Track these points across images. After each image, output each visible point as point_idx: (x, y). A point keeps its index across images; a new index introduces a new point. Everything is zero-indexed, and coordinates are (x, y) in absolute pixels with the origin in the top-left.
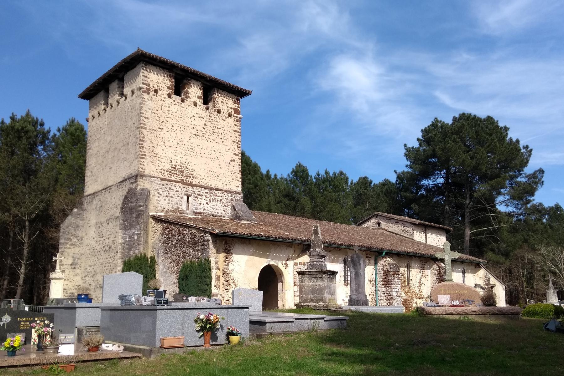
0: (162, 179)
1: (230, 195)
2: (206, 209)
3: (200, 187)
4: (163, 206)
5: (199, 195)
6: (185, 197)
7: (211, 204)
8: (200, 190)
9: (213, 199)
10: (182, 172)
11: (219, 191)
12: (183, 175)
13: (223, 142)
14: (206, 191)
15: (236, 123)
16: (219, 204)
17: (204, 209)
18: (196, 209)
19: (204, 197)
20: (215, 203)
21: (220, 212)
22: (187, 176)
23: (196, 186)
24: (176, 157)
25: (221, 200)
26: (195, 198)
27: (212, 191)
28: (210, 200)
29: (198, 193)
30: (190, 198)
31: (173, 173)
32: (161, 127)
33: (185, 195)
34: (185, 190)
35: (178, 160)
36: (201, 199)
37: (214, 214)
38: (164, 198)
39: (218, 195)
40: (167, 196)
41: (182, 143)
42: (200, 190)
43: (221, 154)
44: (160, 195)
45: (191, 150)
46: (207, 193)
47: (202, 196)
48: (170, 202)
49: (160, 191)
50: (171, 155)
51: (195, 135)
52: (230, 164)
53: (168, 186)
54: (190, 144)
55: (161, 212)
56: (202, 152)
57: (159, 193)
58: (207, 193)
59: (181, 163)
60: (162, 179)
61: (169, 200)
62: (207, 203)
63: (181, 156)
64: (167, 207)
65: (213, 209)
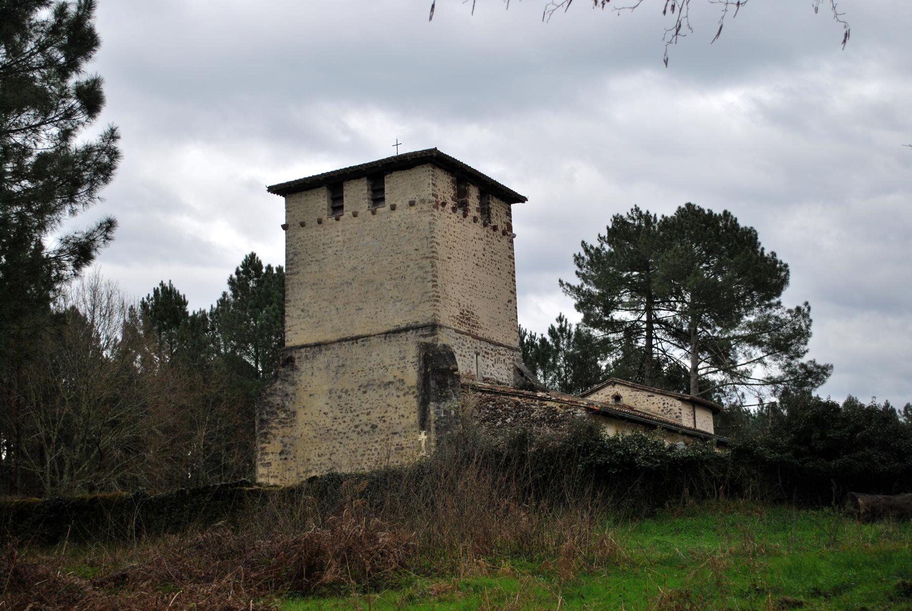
0: (457, 331)
1: (511, 353)
12: (469, 324)
14: (492, 347)
16: (503, 366)
17: (491, 374)
19: (490, 355)
20: (499, 365)
22: (473, 326)
27: (497, 348)
36: (488, 358)
37: (500, 380)
39: (502, 352)
41: (466, 277)
47: (488, 354)
50: (459, 296)
51: (477, 264)
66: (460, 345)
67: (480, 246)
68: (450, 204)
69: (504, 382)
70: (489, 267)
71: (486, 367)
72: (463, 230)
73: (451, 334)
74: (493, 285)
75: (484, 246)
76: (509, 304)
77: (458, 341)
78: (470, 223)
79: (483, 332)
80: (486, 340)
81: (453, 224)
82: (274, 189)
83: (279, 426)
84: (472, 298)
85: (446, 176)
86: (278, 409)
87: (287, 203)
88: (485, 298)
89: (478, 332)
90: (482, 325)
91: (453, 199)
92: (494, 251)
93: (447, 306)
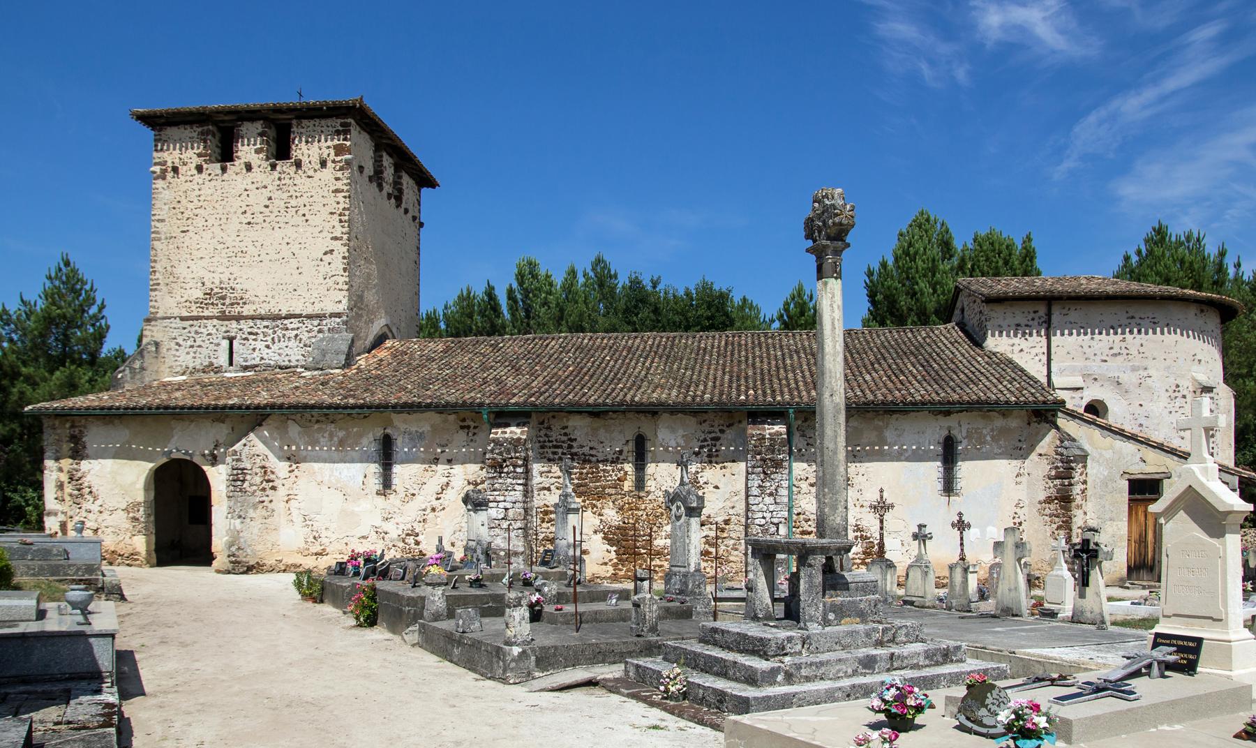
0: (183, 319)
1: (316, 323)
2: (265, 357)
3: (253, 319)
4: (184, 364)
5: (250, 333)
6: (225, 343)
7: (275, 347)
8: (252, 324)
9: (279, 337)
10: (223, 298)
11: (292, 320)
12: (224, 304)
13: (307, 221)
14: (265, 323)
15: (339, 174)
16: (292, 343)
17: (262, 358)
18: (244, 361)
19: (261, 337)
20: (282, 344)
21: (293, 358)
22: (232, 304)
23: (246, 318)
24: (211, 275)
25: (296, 336)
26: (242, 342)
27: (279, 322)
28: (273, 339)
29: (249, 330)
30: (235, 342)
31: (206, 304)
33: (224, 338)
34: (224, 329)
35: (213, 280)
36: (255, 340)
37: (283, 364)
38: (187, 350)
40: (192, 347)
41: (222, 246)
42: (252, 324)
43: (303, 247)
44: (180, 346)
45: (240, 254)
46: (267, 327)
47: (257, 334)
48: (198, 355)
49: (180, 340)
50: (202, 273)
52: (321, 260)
53: (193, 329)
54: (237, 244)
55: (183, 374)
56: (263, 253)
57: (177, 344)
58: (267, 327)
59: (221, 283)
60: (183, 319)
61: (195, 353)
62: (268, 347)
63: (220, 269)
64: (191, 365)
65: (279, 355)
66: (193, 334)
70: (278, 219)
71: (250, 351)
73: (173, 325)
77: (186, 331)
80: (253, 318)
84: (234, 269)
89: (241, 310)
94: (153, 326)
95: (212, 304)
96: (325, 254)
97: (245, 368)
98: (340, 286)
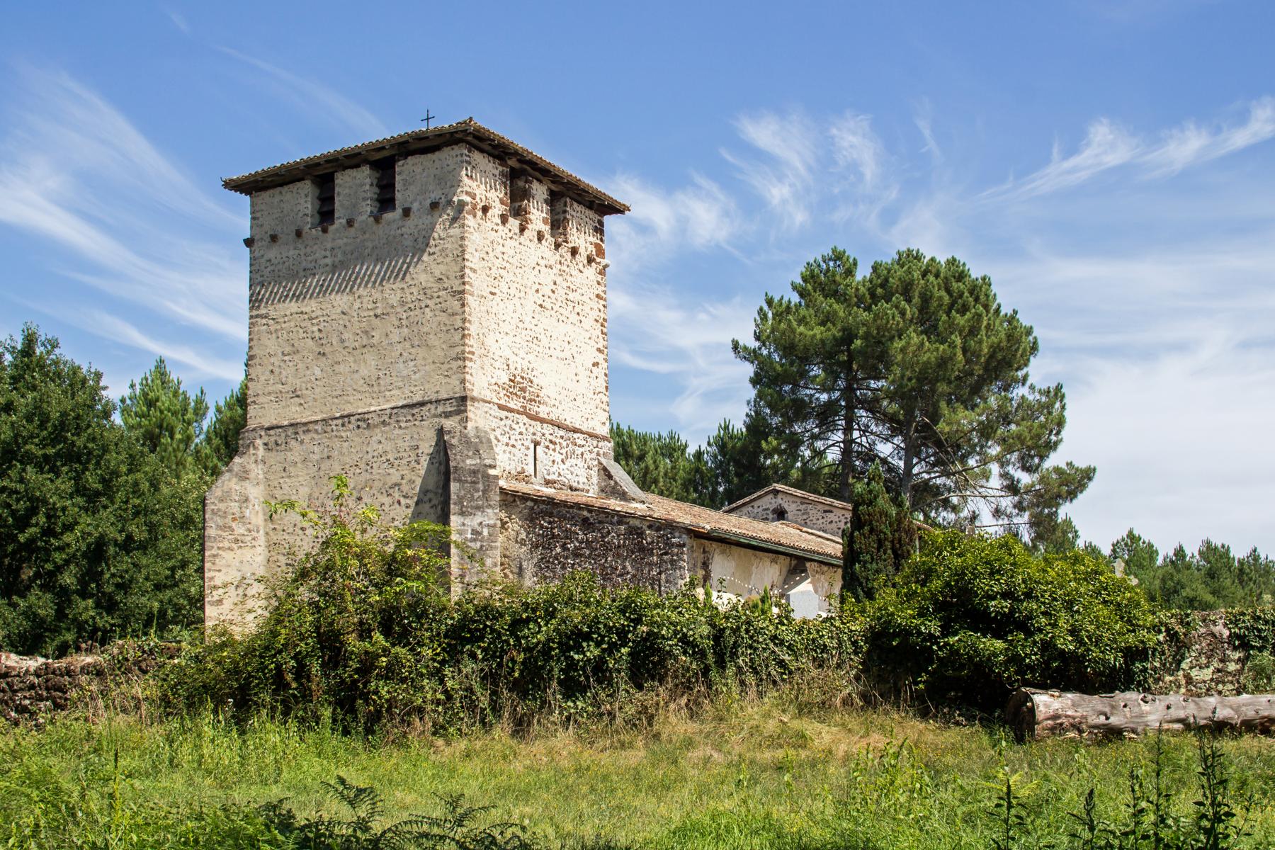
0: (501, 407)
1: (595, 443)
6: (532, 446)
11: (579, 435)
12: (524, 398)
14: (562, 433)
16: (580, 462)
17: (560, 474)
19: (558, 447)
20: (574, 461)
22: (531, 400)
27: (570, 434)
32: (494, 290)
35: (518, 364)
36: (554, 450)
37: (575, 485)
39: (579, 442)
41: (520, 325)
46: (562, 437)
47: (555, 443)
50: (508, 353)
51: (541, 306)
53: (509, 422)
65: (572, 474)
66: (507, 429)
67: (547, 277)
68: (497, 209)
69: (581, 486)
70: (561, 310)
71: (551, 464)
72: (518, 251)
74: (567, 339)
75: (555, 278)
76: (594, 369)
77: (503, 423)
78: (531, 241)
79: (547, 409)
80: (552, 423)
81: (501, 241)
82: (233, 184)
83: (235, 546)
84: (531, 357)
85: (491, 165)
86: (234, 519)
87: (252, 205)
88: (554, 358)
89: (538, 410)
90: (546, 399)
91: (502, 202)
92: (572, 287)
93: (486, 367)
94: (476, 408)
95: (516, 394)
96: (594, 365)
97: (548, 483)
98: (604, 406)
